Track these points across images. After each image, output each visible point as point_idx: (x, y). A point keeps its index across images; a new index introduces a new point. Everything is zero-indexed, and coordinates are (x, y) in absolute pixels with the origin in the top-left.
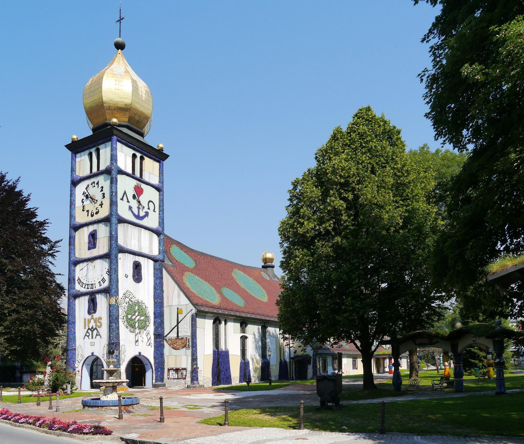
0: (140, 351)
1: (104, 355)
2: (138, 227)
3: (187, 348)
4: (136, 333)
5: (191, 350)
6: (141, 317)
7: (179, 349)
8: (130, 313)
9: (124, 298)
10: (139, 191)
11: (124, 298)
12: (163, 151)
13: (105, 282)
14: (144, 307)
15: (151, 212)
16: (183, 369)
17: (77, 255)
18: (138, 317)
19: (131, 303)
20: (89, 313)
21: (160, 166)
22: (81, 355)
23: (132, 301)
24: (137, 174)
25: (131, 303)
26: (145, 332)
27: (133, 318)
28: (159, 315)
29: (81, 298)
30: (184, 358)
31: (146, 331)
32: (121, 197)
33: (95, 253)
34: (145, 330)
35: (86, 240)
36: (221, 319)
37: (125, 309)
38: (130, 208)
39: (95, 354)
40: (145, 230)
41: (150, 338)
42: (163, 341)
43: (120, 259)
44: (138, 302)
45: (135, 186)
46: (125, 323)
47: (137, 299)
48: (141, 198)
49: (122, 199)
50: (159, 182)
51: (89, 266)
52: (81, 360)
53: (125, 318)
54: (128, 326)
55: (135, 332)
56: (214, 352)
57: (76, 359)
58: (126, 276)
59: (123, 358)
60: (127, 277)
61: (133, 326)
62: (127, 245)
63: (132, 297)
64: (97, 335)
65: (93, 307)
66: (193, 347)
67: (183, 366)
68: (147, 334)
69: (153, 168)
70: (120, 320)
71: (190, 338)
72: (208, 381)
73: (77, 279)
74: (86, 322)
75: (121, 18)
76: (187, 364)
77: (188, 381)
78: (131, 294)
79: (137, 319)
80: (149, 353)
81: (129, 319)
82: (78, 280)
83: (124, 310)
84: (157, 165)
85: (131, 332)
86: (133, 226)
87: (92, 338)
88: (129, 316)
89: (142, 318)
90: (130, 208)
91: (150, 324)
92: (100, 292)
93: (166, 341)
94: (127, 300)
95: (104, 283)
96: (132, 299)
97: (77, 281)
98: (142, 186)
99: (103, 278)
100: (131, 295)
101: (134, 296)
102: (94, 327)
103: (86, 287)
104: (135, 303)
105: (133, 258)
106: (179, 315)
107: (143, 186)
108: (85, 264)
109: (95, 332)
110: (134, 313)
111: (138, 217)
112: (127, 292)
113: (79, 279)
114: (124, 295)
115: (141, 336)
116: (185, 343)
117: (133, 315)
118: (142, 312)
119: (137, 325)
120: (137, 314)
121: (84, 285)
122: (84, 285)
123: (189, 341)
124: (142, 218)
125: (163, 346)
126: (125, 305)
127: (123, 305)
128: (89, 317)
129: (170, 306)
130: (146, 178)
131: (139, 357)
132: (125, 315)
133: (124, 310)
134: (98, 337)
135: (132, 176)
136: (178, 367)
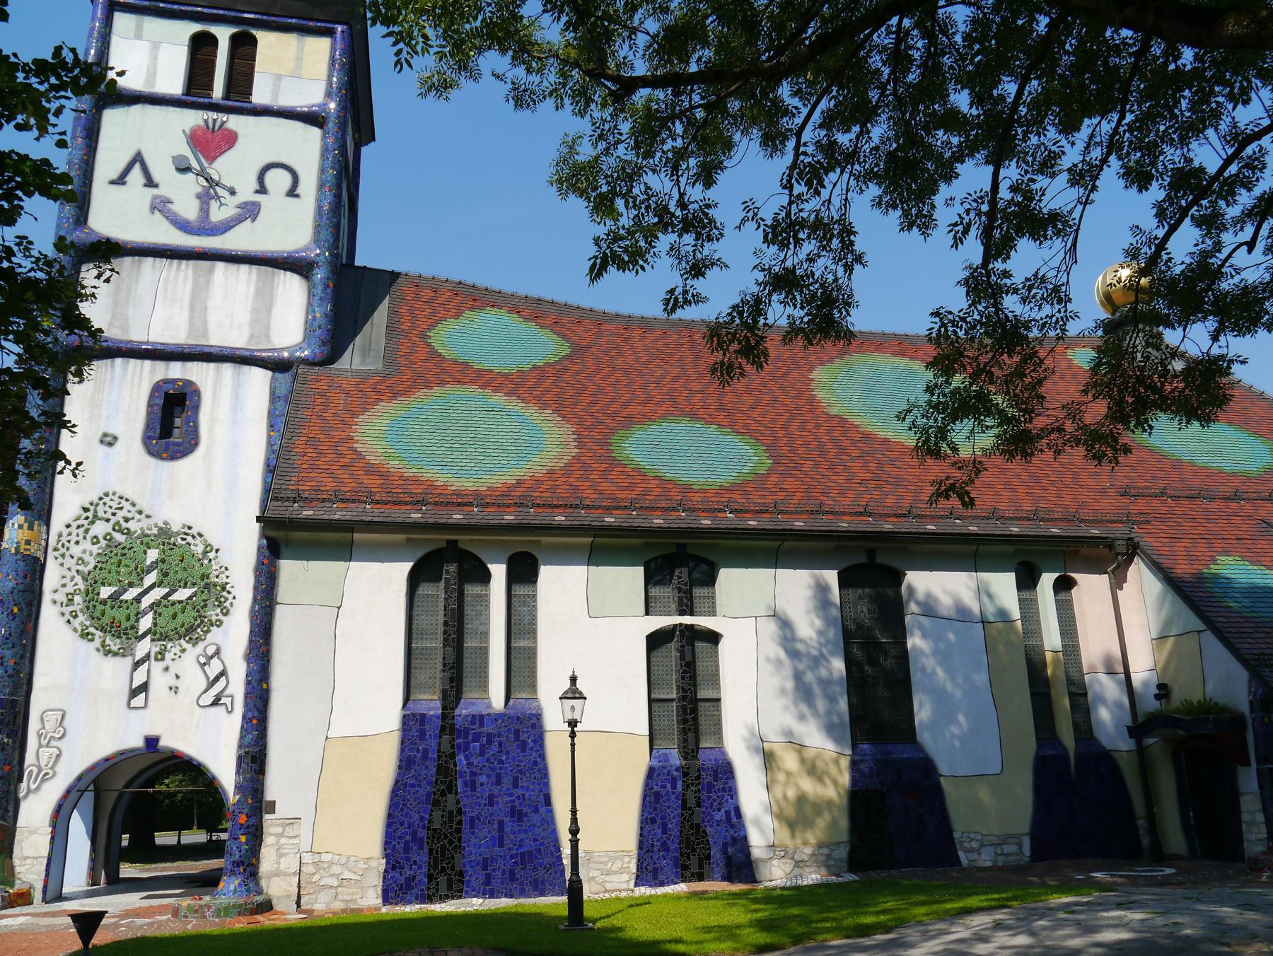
4: (139, 655)
9: (86, 522)
11: (81, 522)
14: (200, 549)
18: (157, 594)
23: (128, 532)
25: (119, 537)
26: (193, 653)
31: (201, 645)
32: (114, 176)
34: (198, 639)
36: (483, 556)
38: (160, 206)
40: (233, 268)
46: (76, 623)
47: (159, 519)
49: (120, 180)
53: (78, 599)
54: (92, 630)
59: (43, 764)
62: (125, 328)
63: (130, 515)
72: (347, 875)
78: (124, 503)
79: (146, 601)
81: (104, 602)
83: (81, 568)
85: (108, 652)
86: (164, 262)
89: (182, 594)
90: (160, 206)
94: (100, 529)
96: (132, 525)
101: (140, 512)
104: (148, 536)
105: (153, 372)
110: (134, 578)
112: (106, 500)
115: (167, 669)
117: (131, 585)
119: (146, 623)
120: (150, 579)
126: (87, 551)
127: (76, 550)
132: (82, 586)
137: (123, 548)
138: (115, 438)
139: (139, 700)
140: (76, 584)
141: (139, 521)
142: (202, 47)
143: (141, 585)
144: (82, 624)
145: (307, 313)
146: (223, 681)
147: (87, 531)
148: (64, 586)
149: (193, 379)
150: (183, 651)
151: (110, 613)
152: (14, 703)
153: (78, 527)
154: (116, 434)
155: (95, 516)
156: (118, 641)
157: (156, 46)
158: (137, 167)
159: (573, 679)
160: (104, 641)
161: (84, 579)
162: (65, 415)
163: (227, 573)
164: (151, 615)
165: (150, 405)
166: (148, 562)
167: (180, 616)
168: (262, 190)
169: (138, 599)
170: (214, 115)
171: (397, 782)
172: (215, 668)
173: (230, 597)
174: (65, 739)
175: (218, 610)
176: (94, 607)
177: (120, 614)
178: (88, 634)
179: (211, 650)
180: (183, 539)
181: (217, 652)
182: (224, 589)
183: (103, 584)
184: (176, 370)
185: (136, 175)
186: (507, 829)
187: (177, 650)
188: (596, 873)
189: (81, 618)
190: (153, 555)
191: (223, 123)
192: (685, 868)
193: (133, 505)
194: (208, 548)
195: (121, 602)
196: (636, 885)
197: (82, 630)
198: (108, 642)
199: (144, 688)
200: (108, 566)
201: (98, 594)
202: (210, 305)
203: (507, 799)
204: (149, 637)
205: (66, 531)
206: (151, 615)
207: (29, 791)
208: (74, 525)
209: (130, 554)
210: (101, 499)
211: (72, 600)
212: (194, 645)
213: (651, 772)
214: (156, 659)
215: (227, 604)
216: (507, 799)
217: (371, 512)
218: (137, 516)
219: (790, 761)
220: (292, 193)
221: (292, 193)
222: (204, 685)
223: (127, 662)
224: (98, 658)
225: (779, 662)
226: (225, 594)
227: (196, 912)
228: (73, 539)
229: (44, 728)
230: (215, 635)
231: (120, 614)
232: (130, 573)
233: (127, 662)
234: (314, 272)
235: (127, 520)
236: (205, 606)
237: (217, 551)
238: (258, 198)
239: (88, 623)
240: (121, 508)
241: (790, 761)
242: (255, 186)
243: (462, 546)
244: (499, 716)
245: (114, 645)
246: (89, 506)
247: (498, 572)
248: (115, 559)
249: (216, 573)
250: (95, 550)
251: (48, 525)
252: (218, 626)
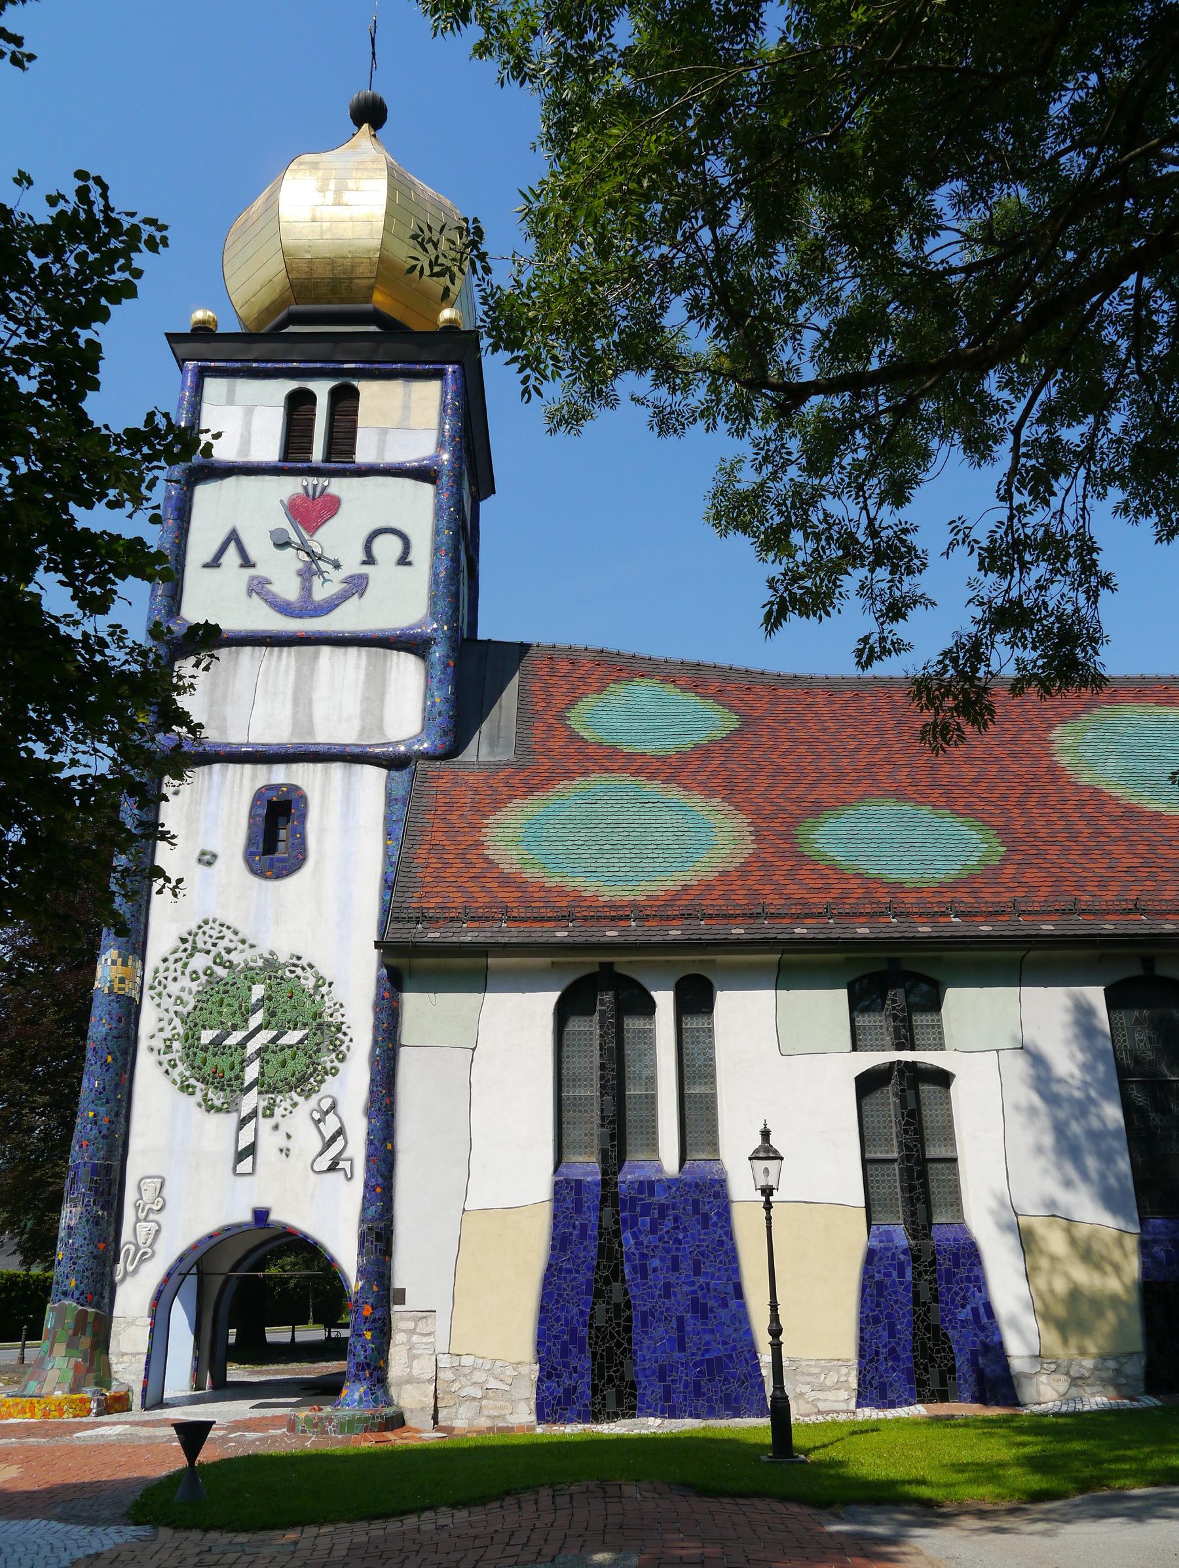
0: (262, 1204)
4: (245, 1111)
9: (184, 955)
11: (179, 955)
14: (311, 983)
18: (264, 1037)
23: (230, 966)
25: (221, 972)
26: (306, 1107)
27: (234, 1039)
31: (315, 1098)
36: (645, 981)
38: (259, 588)
40: (339, 651)
44: (271, 964)
46: (175, 1073)
47: (264, 949)
53: (176, 1045)
54: (192, 1081)
59: (141, 1241)
63: (232, 946)
72: (492, 1384)
79: (252, 1046)
81: (205, 1049)
83: (180, 1009)
85: (210, 1108)
89: (292, 1037)
90: (259, 588)
94: (200, 962)
96: (235, 957)
101: (243, 942)
104: (252, 969)
105: (254, 778)
110: (238, 1019)
112: (206, 928)
114: (184, 941)
115: (276, 1127)
117: (235, 1027)
119: (252, 1072)
120: (256, 1020)
126: (185, 988)
127: (174, 988)
132: (180, 1030)
133: (180, 1009)
137: (225, 985)
138: (215, 856)
140: (174, 1028)
141: (242, 951)
142: (299, 404)
143: (245, 1027)
144: (181, 1074)
145: (425, 698)
146: (340, 1142)
147: (185, 965)
148: (161, 1030)
149: (299, 783)
150: (295, 1105)
151: (212, 1061)
152: (108, 1168)
153: (176, 961)
154: (216, 850)
155: (194, 948)
156: (222, 1094)
157: (249, 410)
158: (232, 547)
159: (766, 1134)
160: (206, 1095)
161: (184, 1022)
162: (179, 776)
163: (342, 1011)
164: (257, 1063)
165: (252, 816)
166: (253, 1000)
167: (290, 1062)
168: (370, 560)
169: (243, 1044)
170: (312, 481)
171: (549, 1267)
172: (331, 1125)
173: (347, 1039)
174: (164, 1212)
175: (333, 1056)
176: (195, 1054)
177: (223, 1063)
178: (188, 1086)
179: (326, 1104)
180: (292, 972)
181: (333, 1107)
182: (339, 1030)
183: (204, 1027)
184: (280, 774)
185: (231, 556)
186: (689, 1329)
187: (287, 1104)
188: (805, 1389)
189: (181, 1067)
190: (258, 991)
191: (325, 488)
192: (921, 1383)
193: (236, 933)
194: (320, 981)
195: (224, 1047)
196: (858, 1405)
197: (182, 1082)
198: (210, 1095)
199: (251, 1150)
200: (209, 1005)
201: (199, 1039)
202: (316, 696)
203: (686, 1288)
204: (255, 1090)
205: (162, 966)
206: (257, 1063)
207: (126, 1273)
208: (172, 958)
209: (233, 990)
210: (200, 927)
211: (170, 1047)
212: (307, 1098)
213: (871, 1256)
214: (264, 1116)
215: (343, 1048)
216: (686, 1288)
217: (508, 932)
218: (240, 946)
219: (1055, 1241)
220: (404, 561)
221: (404, 561)
222: (319, 1146)
223: (233, 1119)
224: (199, 1114)
225: (1032, 1112)
226: (340, 1035)
227: (315, 1425)
228: (171, 975)
229: (141, 1198)
230: (330, 1086)
231: (223, 1063)
232: (234, 1014)
233: (233, 1119)
234: (432, 650)
235: (229, 951)
236: (318, 1051)
237: (330, 984)
238: (366, 569)
239: (188, 1073)
240: (222, 938)
241: (1055, 1241)
242: (362, 557)
243: (619, 970)
244: (673, 1182)
245: (217, 1099)
246: (186, 936)
247: (665, 1000)
248: (217, 998)
249: (330, 1011)
250: (195, 986)
251: (143, 959)
252: (334, 1075)
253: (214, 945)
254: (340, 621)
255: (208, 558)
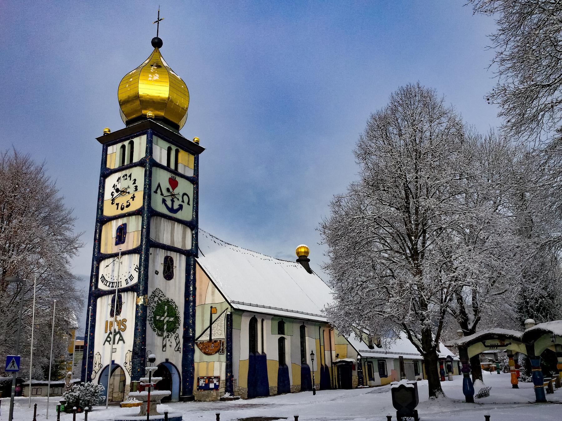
1: (126, 363)
2: (171, 221)
3: (220, 352)
5: (225, 355)
6: (169, 319)
7: (211, 354)
8: (159, 313)
10: (174, 183)
11: (152, 297)
12: (199, 144)
13: (132, 279)
14: (174, 306)
15: (185, 205)
16: (215, 377)
17: (103, 251)
18: (167, 319)
19: (159, 301)
20: (112, 315)
21: (195, 158)
22: (99, 364)
24: (172, 166)
25: (160, 302)
26: (174, 335)
28: (190, 315)
29: (103, 297)
30: (217, 364)
31: (175, 334)
33: (123, 247)
35: (114, 234)
37: (154, 309)
39: (116, 362)
41: (179, 342)
42: (193, 346)
43: (151, 254)
44: (168, 301)
45: (170, 179)
47: (167, 297)
48: (176, 191)
50: (194, 175)
51: (115, 262)
52: (99, 370)
53: (152, 319)
55: (163, 336)
56: (250, 356)
57: (92, 369)
58: (157, 273)
60: (157, 274)
61: (161, 329)
62: (159, 239)
63: (161, 295)
64: (119, 340)
65: (116, 309)
66: (228, 351)
67: (216, 374)
68: (176, 338)
69: (188, 161)
70: (148, 322)
71: (224, 341)
73: (100, 276)
74: (108, 325)
75: (159, 19)
76: (220, 372)
77: (221, 392)
79: (165, 321)
80: (177, 360)
82: (102, 277)
84: (192, 158)
85: (159, 335)
87: (114, 343)
88: (158, 318)
89: (172, 319)
90: (164, 201)
91: (179, 325)
92: (126, 290)
93: (197, 345)
94: (156, 299)
95: (131, 281)
96: (162, 298)
97: (101, 279)
98: (177, 179)
99: (131, 275)
100: (161, 293)
101: (163, 295)
102: (117, 331)
103: (111, 285)
104: (165, 302)
105: (164, 253)
106: (213, 315)
107: (178, 179)
108: (111, 260)
109: (118, 337)
110: (163, 314)
111: (171, 210)
112: (157, 290)
113: (103, 277)
114: (153, 293)
115: (169, 340)
116: (219, 347)
118: (172, 312)
119: (165, 327)
120: (166, 314)
121: (108, 283)
122: (108, 283)
123: (223, 345)
124: (176, 211)
125: (193, 351)
128: (112, 319)
129: (203, 305)
130: (180, 170)
131: (166, 365)
134: (121, 342)
135: (167, 168)
136: (210, 375)
139: (164, 349)
142: (169, 150)
144: (153, 327)
145: (192, 240)
146: (179, 345)
147: (153, 300)
148: (150, 315)
150: (172, 335)
152: (378, 360)
153: (152, 298)
154: (159, 271)
159: (312, 351)
161: (154, 314)
169: (163, 321)
172: (177, 341)
177: (160, 324)
179: (177, 335)
182: (179, 318)
184: (169, 254)
185: (159, 191)
191: (175, 178)
193: (162, 292)
210: (156, 290)
211: (151, 320)
213: (279, 369)
220: (188, 204)
221: (188, 204)
224: (156, 336)
230: (177, 332)
231: (160, 324)
233: (161, 338)
235: (161, 297)
238: (182, 203)
240: (160, 293)
253: (158, 295)
254: (179, 215)
255: (155, 190)
